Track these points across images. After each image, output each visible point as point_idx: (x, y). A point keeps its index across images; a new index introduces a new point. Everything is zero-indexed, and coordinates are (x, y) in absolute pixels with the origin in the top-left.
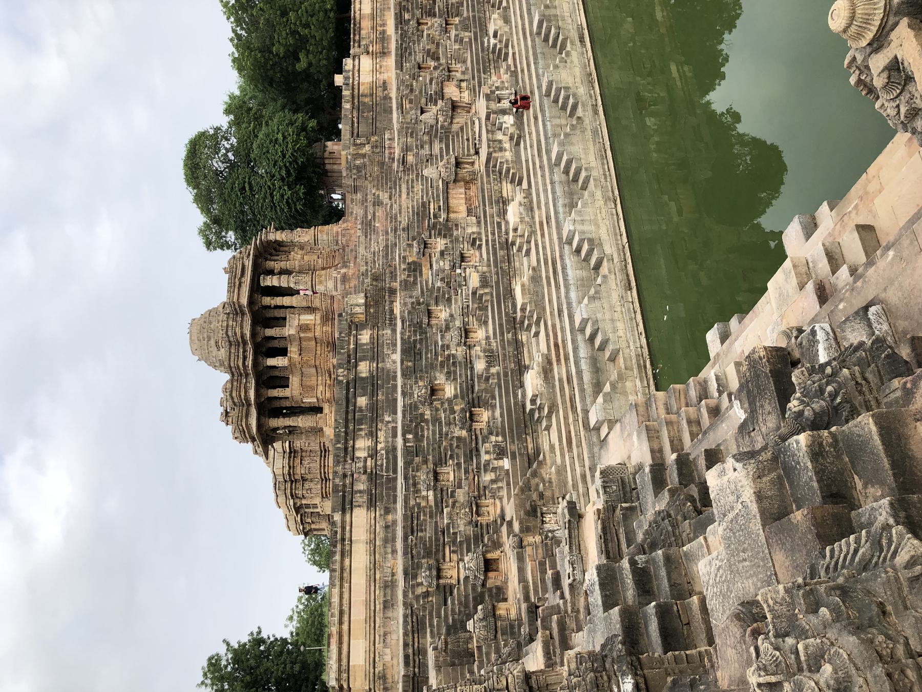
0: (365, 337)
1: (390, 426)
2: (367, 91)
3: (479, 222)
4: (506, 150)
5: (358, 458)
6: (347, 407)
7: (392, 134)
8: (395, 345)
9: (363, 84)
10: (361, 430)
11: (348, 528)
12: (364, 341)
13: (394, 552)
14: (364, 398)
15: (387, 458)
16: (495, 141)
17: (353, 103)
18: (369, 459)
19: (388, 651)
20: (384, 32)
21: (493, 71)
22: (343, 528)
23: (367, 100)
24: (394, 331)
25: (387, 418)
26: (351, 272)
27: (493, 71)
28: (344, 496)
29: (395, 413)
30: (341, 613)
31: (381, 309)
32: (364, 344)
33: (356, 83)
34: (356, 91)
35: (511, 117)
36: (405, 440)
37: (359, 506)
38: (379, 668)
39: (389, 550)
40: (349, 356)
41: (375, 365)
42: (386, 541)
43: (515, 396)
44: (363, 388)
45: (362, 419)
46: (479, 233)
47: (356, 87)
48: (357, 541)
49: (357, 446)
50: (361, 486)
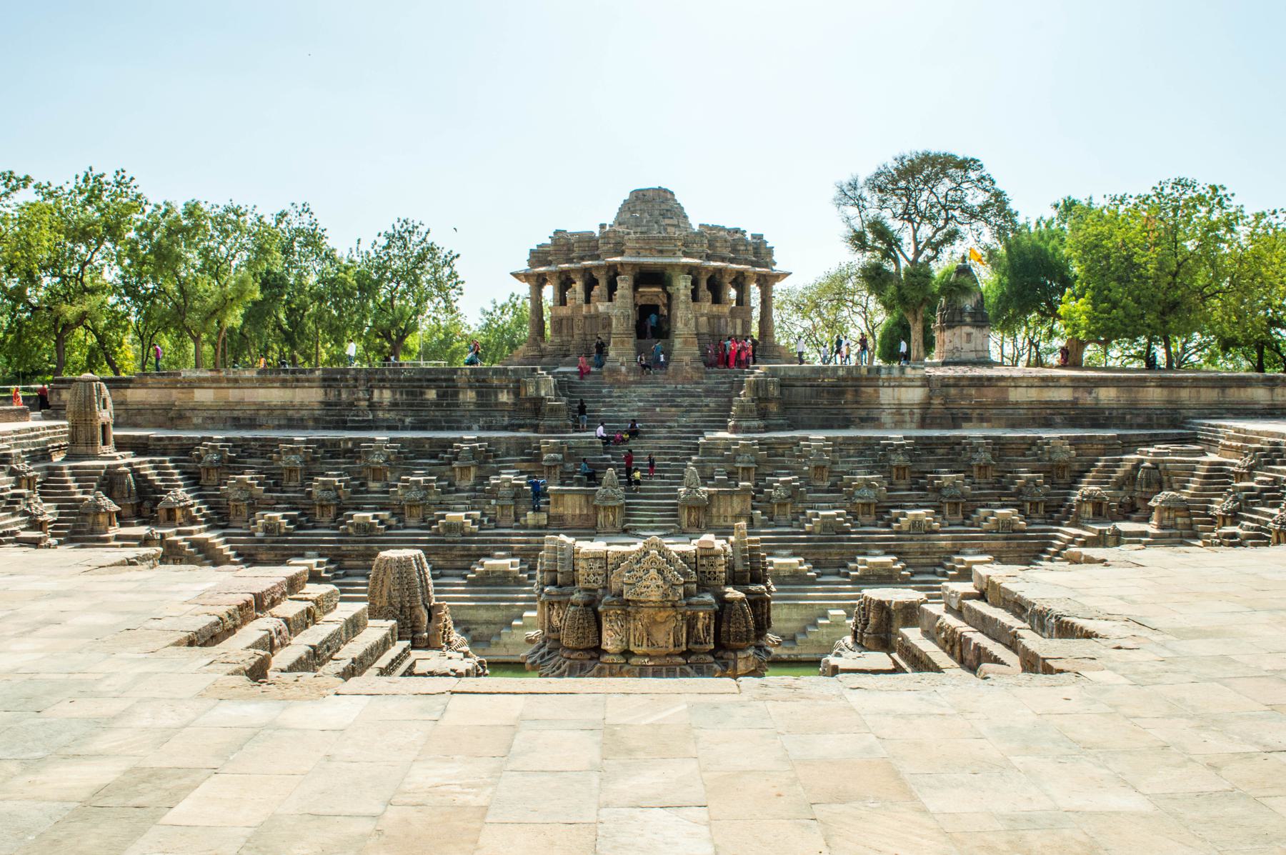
1: (399, 425)
2: (863, 398)
3: (540, 527)
6: (429, 380)
7: (757, 430)
8: (489, 428)
9: (876, 392)
12: (500, 396)
13: (279, 427)
15: (364, 421)
19: (200, 421)
20: (968, 419)
23: (849, 397)
24: (505, 428)
25: (408, 420)
26: (621, 378)
28: (336, 380)
29: (413, 428)
30: (236, 381)
31: (529, 415)
32: (496, 396)
36: (346, 441)
38: (188, 414)
39: (282, 422)
42: (290, 419)
43: (313, 549)
46: (525, 527)
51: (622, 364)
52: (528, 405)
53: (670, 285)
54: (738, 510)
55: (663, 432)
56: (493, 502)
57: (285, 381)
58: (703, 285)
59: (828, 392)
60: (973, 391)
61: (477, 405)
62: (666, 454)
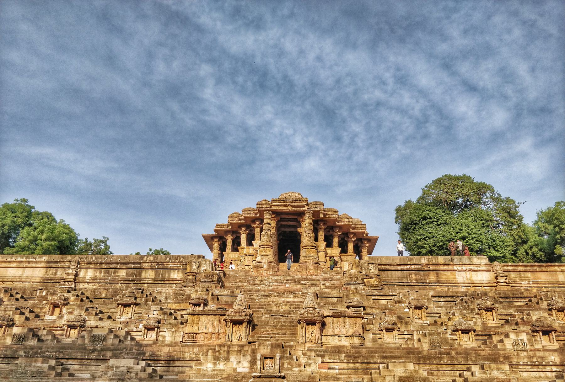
0: (176, 275)
4: (215, 364)
5: (80, 271)
10: (101, 273)
11: (34, 265)
14: (125, 274)
16: (228, 352)
17: (427, 265)
18: (73, 277)
21: (351, 365)
22: (36, 263)
27: (351, 365)
33: (455, 268)
34: (442, 268)
35: (246, 370)
37: (46, 272)
40: (162, 264)
41: (150, 282)
44: (133, 274)
45: (108, 273)
47: (450, 268)
48: (24, 272)
49: (89, 270)
50: (60, 273)
51: (265, 263)
52: (191, 277)
53: (300, 226)
54: (350, 332)
55: (292, 296)
56: (141, 326)
57: (20, 262)
58: (321, 234)
59: (416, 275)
60: (529, 275)
61: (154, 279)
62: (291, 305)
